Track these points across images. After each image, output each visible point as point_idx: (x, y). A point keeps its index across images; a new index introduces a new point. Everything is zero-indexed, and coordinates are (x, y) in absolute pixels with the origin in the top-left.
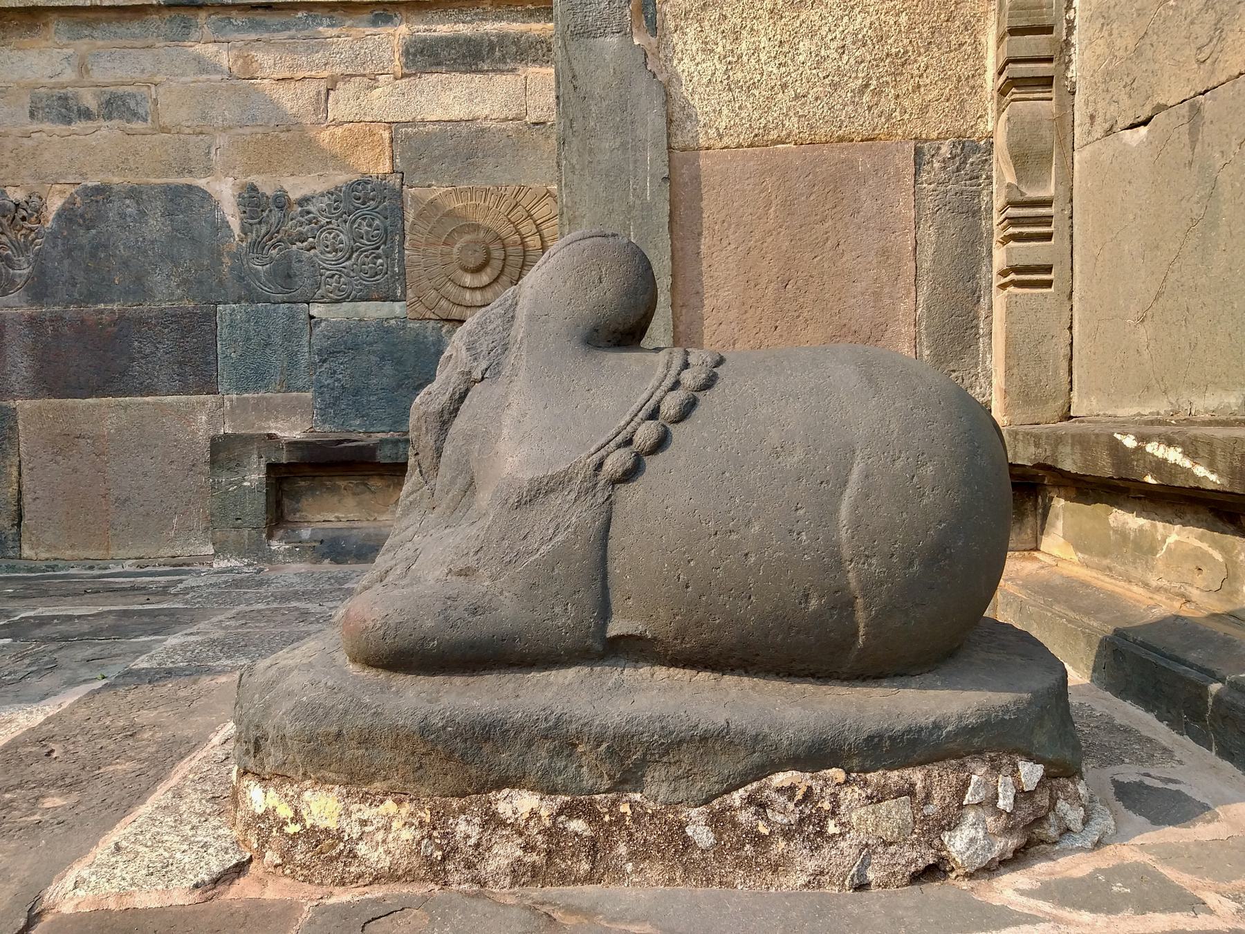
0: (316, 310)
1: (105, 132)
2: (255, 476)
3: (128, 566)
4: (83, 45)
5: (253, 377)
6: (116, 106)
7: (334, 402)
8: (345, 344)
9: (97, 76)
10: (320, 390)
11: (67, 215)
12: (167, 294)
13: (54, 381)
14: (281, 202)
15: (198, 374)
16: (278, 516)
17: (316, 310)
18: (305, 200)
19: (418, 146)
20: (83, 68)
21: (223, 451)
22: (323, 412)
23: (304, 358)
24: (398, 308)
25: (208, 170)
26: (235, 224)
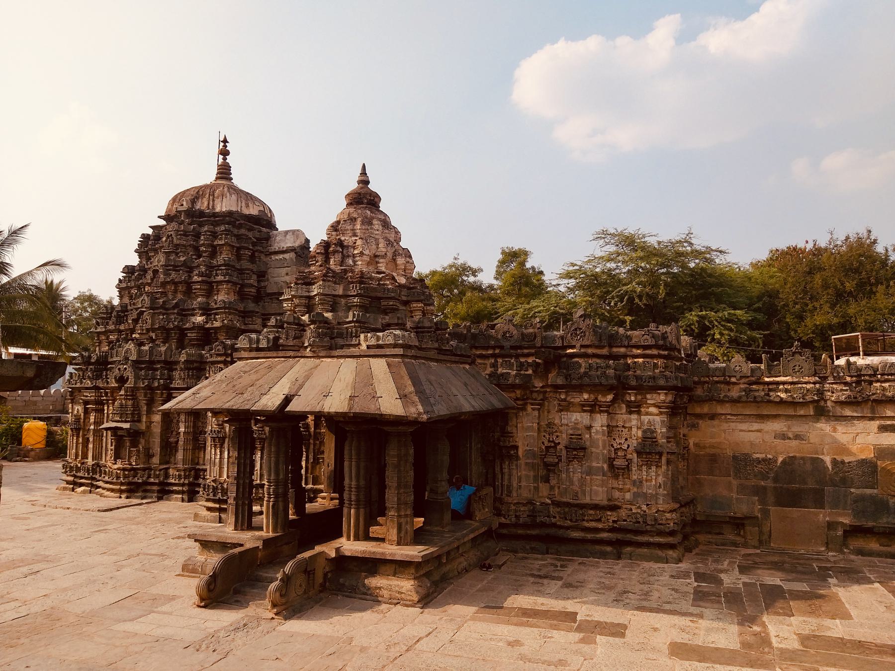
0: (852, 490)
1: (794, 443)
2: (840, 533)
3: (803, 552)
4: (789, 423)
5: (835, 505)
6: (797, 437)
7: (857, 514)
8: (862, 498)
9: (793, 430)
10: (853, 510)
11: (783, 462)
12: (811, 484)
13: (780, 503)
14: (843, 462)
15: (819, 503)
16: (845, 544)
17: (852, 490)
18: (850, 462)
19: (882, 452)
20: (789, 427)
21: (831, 526)
22: (854, 517)
23: (849, 502)
24: (875, 491)
25: (823, 454)
26: (830, 467)
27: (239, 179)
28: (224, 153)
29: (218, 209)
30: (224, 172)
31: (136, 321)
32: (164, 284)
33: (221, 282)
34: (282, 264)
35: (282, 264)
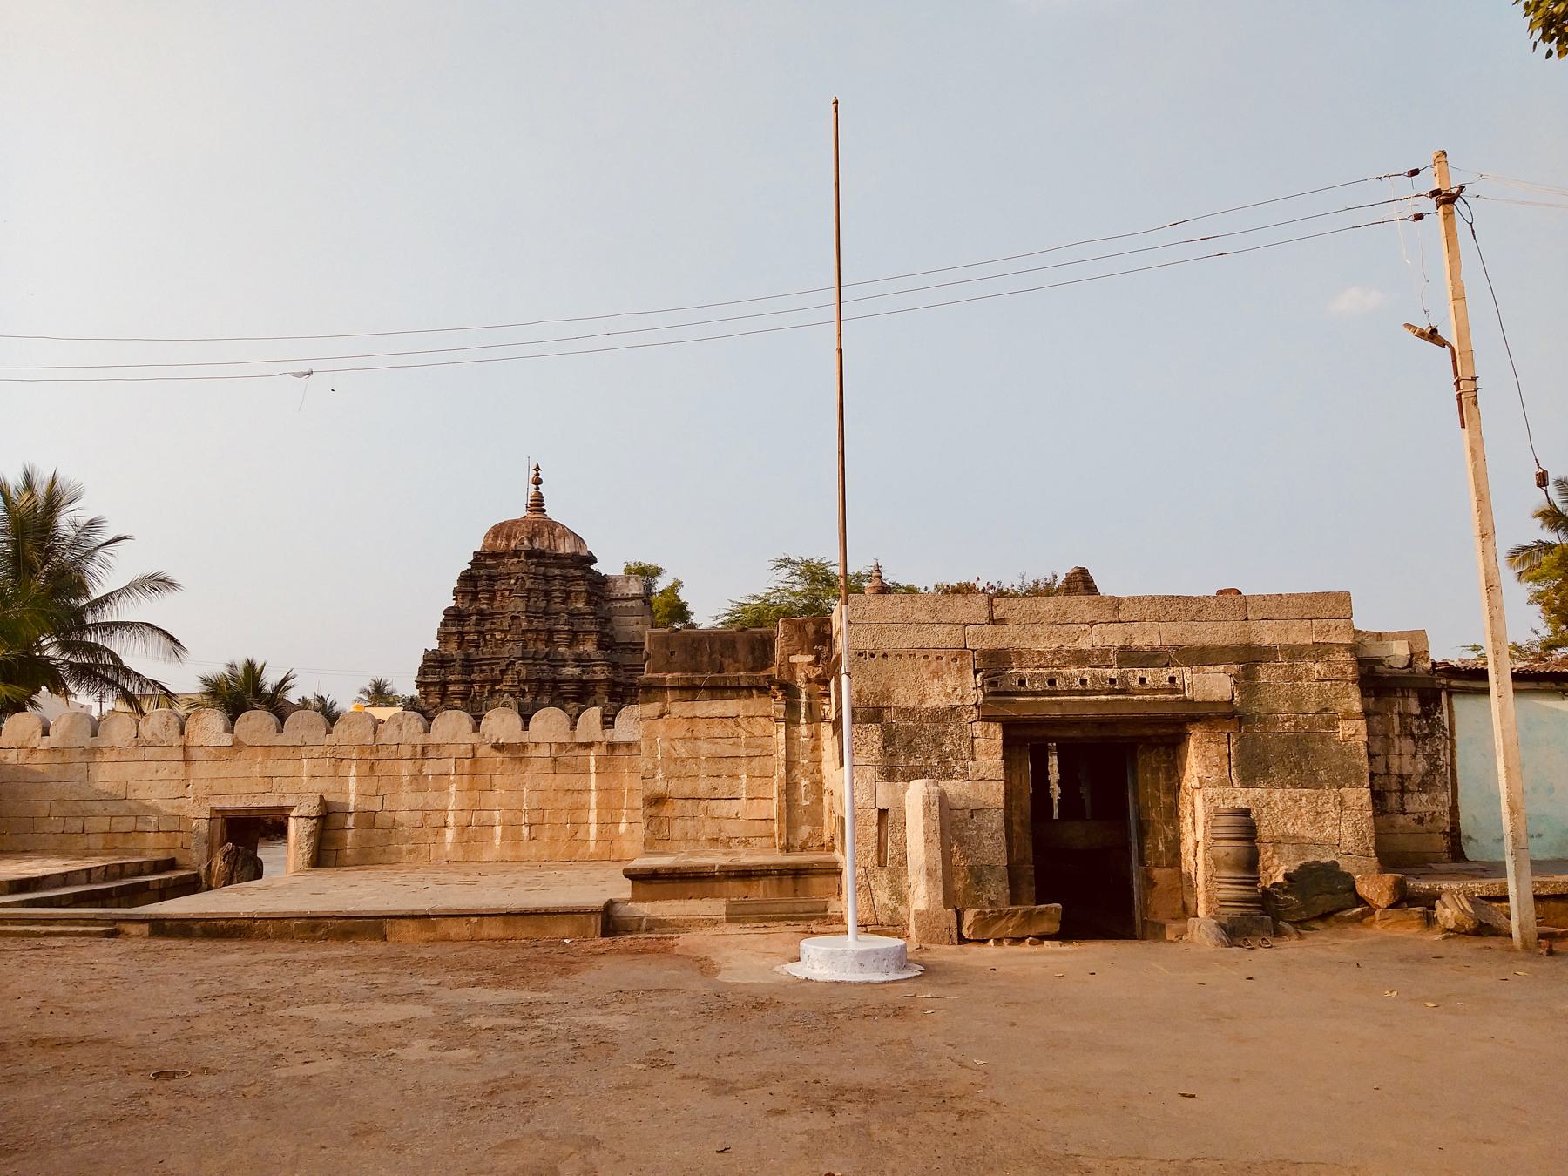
27: (553, 512)
28: (538, 482)
29: (561, 551)
30: (537, 504)
31: (503, 672)
32: (524, 632)
33: (591, 632)
34: (629, 612)
35: (629, 612)
